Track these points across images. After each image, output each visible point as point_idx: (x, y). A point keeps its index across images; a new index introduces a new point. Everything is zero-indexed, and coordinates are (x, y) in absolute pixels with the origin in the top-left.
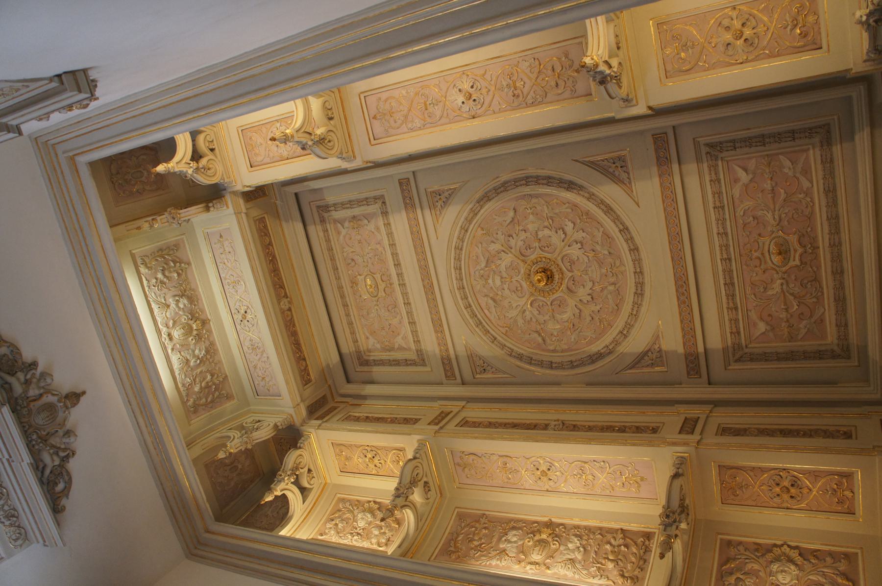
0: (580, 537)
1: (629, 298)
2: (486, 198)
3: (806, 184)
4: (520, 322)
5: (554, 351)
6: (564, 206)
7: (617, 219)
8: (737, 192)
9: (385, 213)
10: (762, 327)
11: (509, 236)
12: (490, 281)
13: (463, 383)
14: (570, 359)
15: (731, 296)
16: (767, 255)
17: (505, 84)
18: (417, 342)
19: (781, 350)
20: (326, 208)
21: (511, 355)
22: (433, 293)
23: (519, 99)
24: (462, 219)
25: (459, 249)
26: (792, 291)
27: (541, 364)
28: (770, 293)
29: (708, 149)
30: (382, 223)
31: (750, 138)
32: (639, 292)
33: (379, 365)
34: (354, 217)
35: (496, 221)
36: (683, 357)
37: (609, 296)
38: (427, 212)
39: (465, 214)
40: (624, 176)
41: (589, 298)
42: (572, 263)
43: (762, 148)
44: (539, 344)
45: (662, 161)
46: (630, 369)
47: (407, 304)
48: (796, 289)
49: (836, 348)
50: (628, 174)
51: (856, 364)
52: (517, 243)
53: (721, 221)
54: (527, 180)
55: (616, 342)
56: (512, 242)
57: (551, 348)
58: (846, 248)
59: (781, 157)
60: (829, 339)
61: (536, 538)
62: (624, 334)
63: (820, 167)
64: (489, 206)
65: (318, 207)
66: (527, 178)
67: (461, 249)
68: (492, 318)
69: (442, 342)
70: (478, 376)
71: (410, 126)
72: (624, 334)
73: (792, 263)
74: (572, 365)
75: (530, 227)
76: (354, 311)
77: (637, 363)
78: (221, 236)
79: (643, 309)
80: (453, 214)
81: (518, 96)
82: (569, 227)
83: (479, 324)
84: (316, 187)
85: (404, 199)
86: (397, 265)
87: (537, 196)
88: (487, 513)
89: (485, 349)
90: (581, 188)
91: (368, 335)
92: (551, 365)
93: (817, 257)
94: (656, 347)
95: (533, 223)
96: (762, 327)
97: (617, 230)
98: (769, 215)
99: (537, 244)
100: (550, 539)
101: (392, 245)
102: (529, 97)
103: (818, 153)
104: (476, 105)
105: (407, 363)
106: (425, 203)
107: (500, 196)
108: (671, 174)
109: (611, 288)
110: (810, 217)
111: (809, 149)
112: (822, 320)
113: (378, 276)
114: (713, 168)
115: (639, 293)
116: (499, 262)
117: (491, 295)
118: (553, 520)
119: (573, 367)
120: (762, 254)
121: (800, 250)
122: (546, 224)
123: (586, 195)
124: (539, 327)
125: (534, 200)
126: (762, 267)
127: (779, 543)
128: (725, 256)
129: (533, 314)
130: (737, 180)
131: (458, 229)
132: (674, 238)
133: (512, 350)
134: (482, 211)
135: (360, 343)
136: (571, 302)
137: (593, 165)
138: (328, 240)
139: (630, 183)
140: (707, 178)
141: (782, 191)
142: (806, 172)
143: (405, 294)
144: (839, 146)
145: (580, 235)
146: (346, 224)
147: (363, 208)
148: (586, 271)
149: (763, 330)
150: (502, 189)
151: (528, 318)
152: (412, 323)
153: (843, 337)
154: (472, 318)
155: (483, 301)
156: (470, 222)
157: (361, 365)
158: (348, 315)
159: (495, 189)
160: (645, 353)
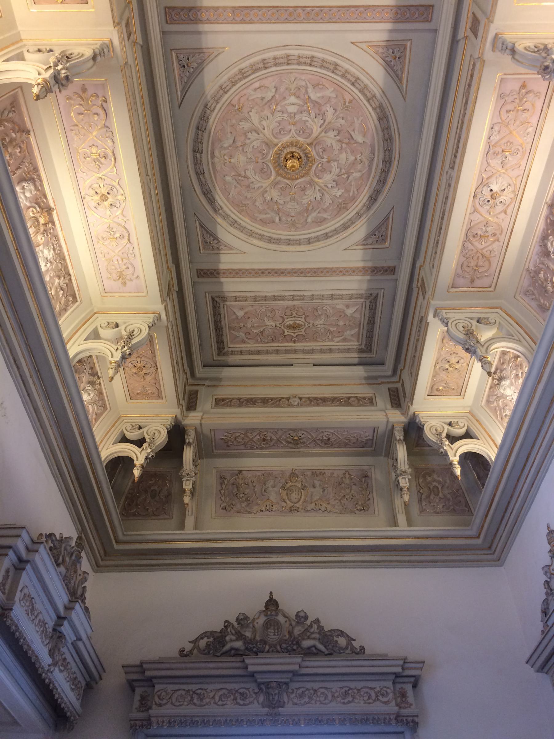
0: (54, 250)
1: (268, 231)
2: (383, 117)
3: (337, 340)
4: (245, 125)
5: (213, 156)
6: (355, 190)
7: (336, 232)
10: (240, 314)
11: (339, 132)
12: (293, 99)
13: (163, 33)
15: (265, 298)
16: (293, 319)
17: (489, 229)
19: (223, 323)
21: (206, 106)
23: (471, 235)
24: (366, 81)
25: (335, 68)
26: (266, 330)
27: (198, 141)
28: (266, 319)
29: (374, 295)
31: (374, 318)
32: (272, 240)
35: (356, 120)
36: (216, 268)
37: (269, 216)
38: (385, 37)
39: (371, 86)
40: (370, 241)
41: (268, 198)
42: (304, 189)
43: (366, 322)
44: (221, 141)
45: (375, 271)
46: (200, 224)
48: (268, 332)
49: (226, 350)
50: (371, 244)
51: (215, 359)
52: (331, 139)
53: (322, 297)
54: (388, 162)
55: (226, 217)
56: (331, 134)
57: (217, 153)
59: (357, 330)
60: (230, 346)
61: (37, 215)
62: (234, 223)
63: (347, 347)
64: (371, 116)
66: (390, 163)
67: (333, 72)
68: (250, 91)
71: (496, 128)
72: (234, 223)
73: (286, 331)
74: (199, 173)
75: (343, 156)
77: (206, 230)
79: (255, 242)
81: (474, 237)
82: (338, 192)
83: (243, 74)
87: (370, 166)
88: (32, 133)
89: (212, 78)
90: (369, 208)
92: (196, 151)
93: (287, 342)
94: (222, 247)
96: (240, 314)
97: (327, 231)
98: (321, 322)
99: (325, 160)
100: (42, 228)
102: (470, 245)
103: (355, 347)
104: (484, 201)
108: (364, 275)
109: (277, 220)
110: (316, 340)
111: (358, 341)
112: (244, 342)
114: (360, 296)
115: (270, 240)
116: (313, 114)
117: (277, 96)
118: (54, 213)
120: (294, 317)
121: (294, 335)
122: (343, 171)
123: (362, 212)
124: (239, 144)
125: (367, 163)
126: (285, 317)
127: (100, 375)
128: (296, 298)
129: (251, 143)
130: (348, 306)
131: (357, 74)
133: (213, 111)
134: (370, 109)
136: (266, 183)
139: (363, 245)
141: (335, 329)
142: (345, 340)
144: (357, 356)
145: (328, 201)
148: (293, 199)
149: (238, 314)
150: (387, 136)
151: (249, 135)
153: (233, 353)
154: (251, 66)
155: (270, 83)
156: (361, 91)
159: (388, 128)
160: (216, 238)
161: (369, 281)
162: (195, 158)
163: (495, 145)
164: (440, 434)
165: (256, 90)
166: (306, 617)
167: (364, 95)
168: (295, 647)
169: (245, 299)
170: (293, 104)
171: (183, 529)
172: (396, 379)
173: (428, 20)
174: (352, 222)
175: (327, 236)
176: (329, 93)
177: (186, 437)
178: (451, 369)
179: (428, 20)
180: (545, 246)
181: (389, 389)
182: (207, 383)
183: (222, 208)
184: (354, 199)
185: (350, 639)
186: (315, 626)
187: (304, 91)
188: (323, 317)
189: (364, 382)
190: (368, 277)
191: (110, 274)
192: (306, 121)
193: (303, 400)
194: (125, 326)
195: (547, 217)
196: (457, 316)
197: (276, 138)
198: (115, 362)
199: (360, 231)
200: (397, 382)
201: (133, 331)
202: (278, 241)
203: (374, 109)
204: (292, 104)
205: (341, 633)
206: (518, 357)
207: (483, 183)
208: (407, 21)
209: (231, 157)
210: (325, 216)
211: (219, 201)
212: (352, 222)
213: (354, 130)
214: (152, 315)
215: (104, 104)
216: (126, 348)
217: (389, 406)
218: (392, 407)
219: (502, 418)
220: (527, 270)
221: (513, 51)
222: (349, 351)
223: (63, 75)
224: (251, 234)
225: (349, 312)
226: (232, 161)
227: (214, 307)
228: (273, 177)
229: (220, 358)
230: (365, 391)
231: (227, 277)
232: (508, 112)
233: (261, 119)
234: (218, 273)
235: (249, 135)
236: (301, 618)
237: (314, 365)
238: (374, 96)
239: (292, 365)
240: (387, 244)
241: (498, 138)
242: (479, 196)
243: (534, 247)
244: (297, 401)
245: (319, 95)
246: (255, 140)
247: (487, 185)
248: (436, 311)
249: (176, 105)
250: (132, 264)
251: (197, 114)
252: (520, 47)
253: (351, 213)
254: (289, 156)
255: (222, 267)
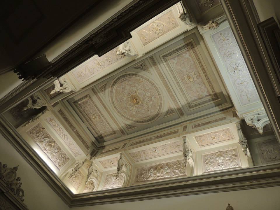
1: (115, 101)
2: (157, 115)
4: (137, 85)
7: (125, 117)
8: (107, 126)
9: (188, 104)
12: (149, 94)
13: (147, 58)
14: (120, 80)
15: (97, 108)
18: (168, 65)
20: (213, 100)
22: (165, 86)
23: (144, 151)
30: (189, 100)
33: (182, 47)
34: (201, 99)
38: (173, 108)
42: (130, 105)
47: (174, 77)
49: (76, 104)
51: (72, 102)
52: (145, 106)
53: (107, 121)
57: (126, 81)
58: (86, 121)
64: (155, 113)
65: (218, 98)
69: (158, 70)
70: (143, 62)
71: (168, 145)
72: (111, 92)
76: (198, 64)
78: (249, 101)
79: (110, 99)
80: (165, 109)
82: (134, 113)
83: (148, 80)
84: (217, 107)
85: (181, 110)
86: (181, 89)
87: (143, 118)
89: (143, 73)
90: (135, 122)
91: (190, 57)
92: (124, 76)
94: (104, 92)
95: (143, 112)
97: (124, 115)
99: (140, 107)
101: (184, 95)
105: (170, 54)
106: (174, 110)
107: (153, 117)
113: (188, 82)
114: (113, 130)
115: (113, 103)
119: (118, 78)
124: (132, 85)
125: (145, 116)
131: (163, 105)
132: (112, 117)
135: (192, 52)
137: (135, 127)
138: (212, 88)
140: (113, 128)
143: (176, 80)
145: (131, 112)
146: (204, 96)
147: (198, 103)
152: (171, 71)
157: (191, 42)
158: (200, 62)
160: (105, 89)
161: (118, 130)
162: (122, 76)
163: (165, 146)
164: (92, 172)
165: (146, 84)
166: (20, 180)
167: (159, 109)
168: (10, 185)
169: (94, 103)
170: (148, 94)
171: (16, 128)
172: (97, 149)
173: (181, 115)
174: (130, 119)
175: (123, 115)
176: (155, 101)
177: (44, 111)
178: (110, 163)
179: (181, 115)
180: (151, 169)
181: (94, 149)
182: (63, 104)
183: (113, 88)
184: (135, 117)
185: (23, 195)
186: (19, 185)
187: (152, 95)
188: (101, 123)
189: (92, 142)
190: (119, 130)
191: (79, 73)
192: (146, 99)
193: (76, 132)
194: (67, 84)
195: (156, 165)
196: (124, 159)
197: (138, 94)
198: (56, 91)
199: (129, 123)
200: (97, 149)
201: (67, 88)
202: (114, 105)
203: (157, 113)
204: (148, 94)
205: (23, 192)
206: (123, 177)
207: (156, 148)
208: (179, 111)
209: (127, 85)
210: (127, 113)
211: (115, 87)
212: (130, 119)
213: (150, 110)
214: (74, 88)
215: (123, 57)
216: (62, 90)
217: (90, 153)
218: (91, 154)
219: (106, 182)
220: (143, 167)
221: (185, 143)
222: (97, 133)
223: (125, 54)
224: (112, 97)
225: (107, 129)
226: (127, 86)
227: (86, 96)
228: (129, 97)
229: (72, 103)
230: (89, 144)
231: (97, 97)
232: (173, 145)
233: (140, 88)
234: (96, 94)
235: (135, 87)
236: (19, 179)
237: (88, 128)
238: (160, 111)
239: (83, 122)
240: (130, 130)
241: (167, 146)
242: (153, 149)
243: (149, 166)
244: (75, 130)
245: (153, 99)
246: (135, 89)
247: (156, 149)
248: (121, 153)
249: (132, 67)
250: (85, 77)
251: (133, 73)
252: (186, 144)
253: (132, 119)
254: (136, 99)
255: (98, 94)
